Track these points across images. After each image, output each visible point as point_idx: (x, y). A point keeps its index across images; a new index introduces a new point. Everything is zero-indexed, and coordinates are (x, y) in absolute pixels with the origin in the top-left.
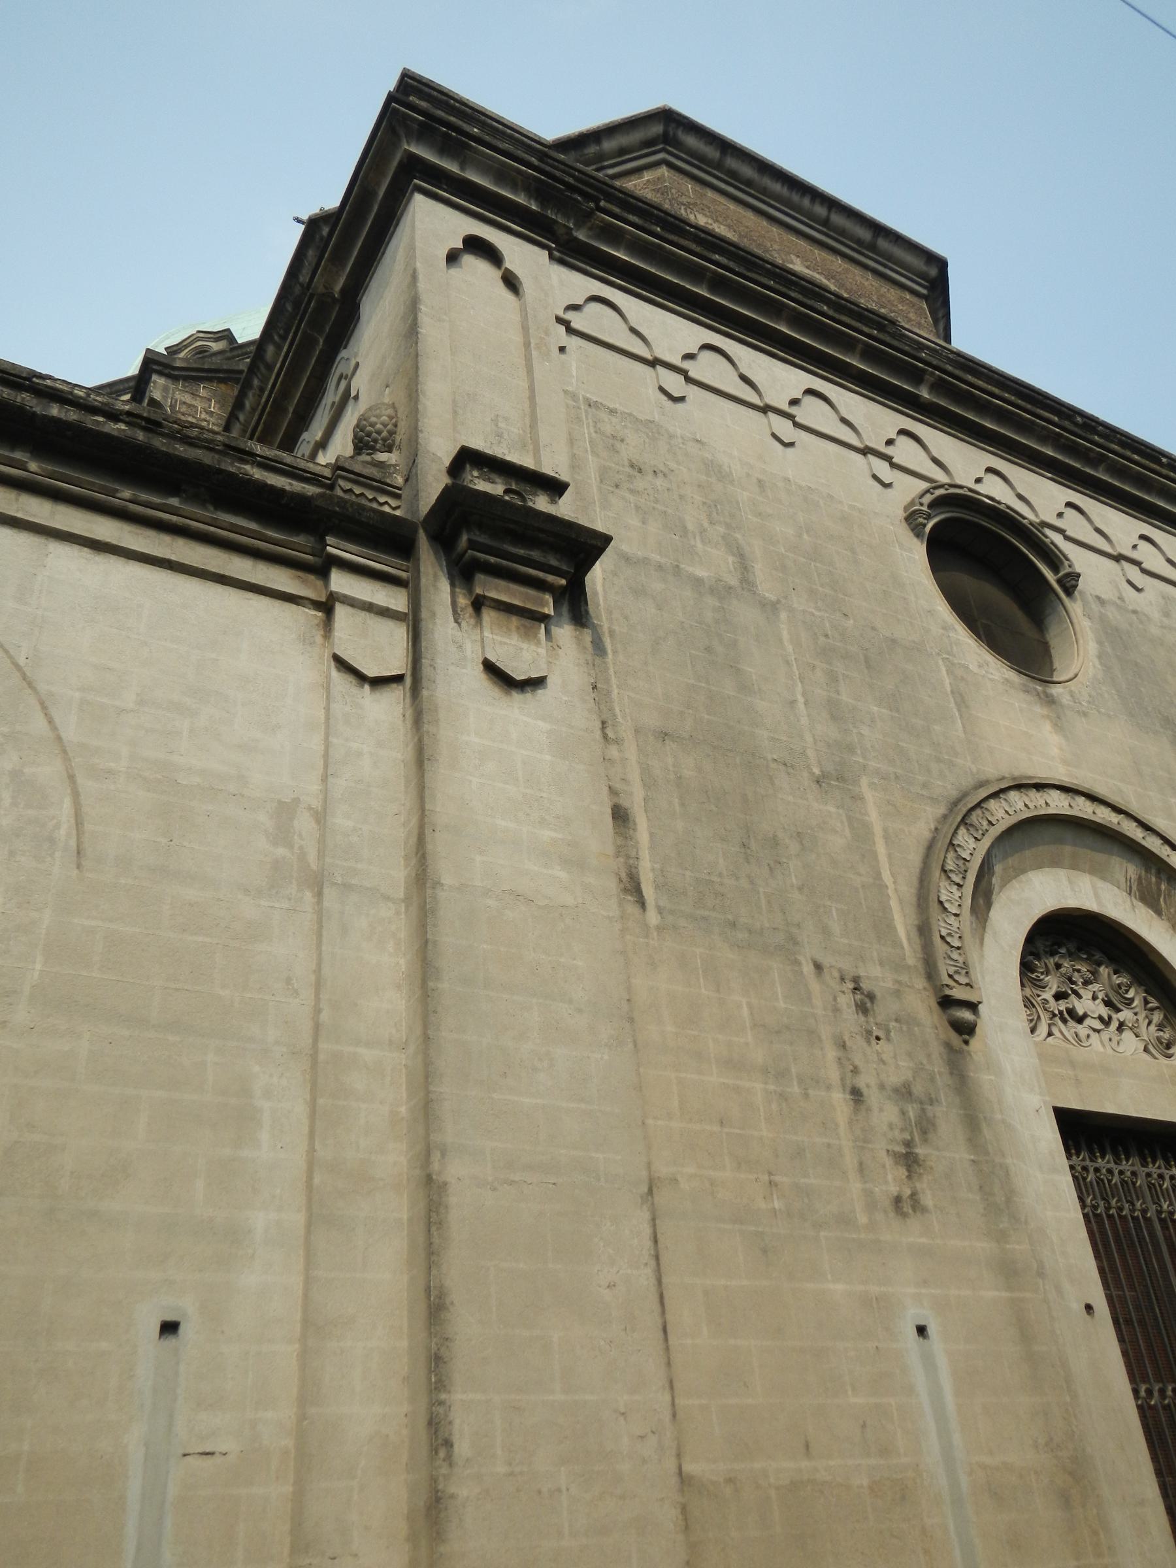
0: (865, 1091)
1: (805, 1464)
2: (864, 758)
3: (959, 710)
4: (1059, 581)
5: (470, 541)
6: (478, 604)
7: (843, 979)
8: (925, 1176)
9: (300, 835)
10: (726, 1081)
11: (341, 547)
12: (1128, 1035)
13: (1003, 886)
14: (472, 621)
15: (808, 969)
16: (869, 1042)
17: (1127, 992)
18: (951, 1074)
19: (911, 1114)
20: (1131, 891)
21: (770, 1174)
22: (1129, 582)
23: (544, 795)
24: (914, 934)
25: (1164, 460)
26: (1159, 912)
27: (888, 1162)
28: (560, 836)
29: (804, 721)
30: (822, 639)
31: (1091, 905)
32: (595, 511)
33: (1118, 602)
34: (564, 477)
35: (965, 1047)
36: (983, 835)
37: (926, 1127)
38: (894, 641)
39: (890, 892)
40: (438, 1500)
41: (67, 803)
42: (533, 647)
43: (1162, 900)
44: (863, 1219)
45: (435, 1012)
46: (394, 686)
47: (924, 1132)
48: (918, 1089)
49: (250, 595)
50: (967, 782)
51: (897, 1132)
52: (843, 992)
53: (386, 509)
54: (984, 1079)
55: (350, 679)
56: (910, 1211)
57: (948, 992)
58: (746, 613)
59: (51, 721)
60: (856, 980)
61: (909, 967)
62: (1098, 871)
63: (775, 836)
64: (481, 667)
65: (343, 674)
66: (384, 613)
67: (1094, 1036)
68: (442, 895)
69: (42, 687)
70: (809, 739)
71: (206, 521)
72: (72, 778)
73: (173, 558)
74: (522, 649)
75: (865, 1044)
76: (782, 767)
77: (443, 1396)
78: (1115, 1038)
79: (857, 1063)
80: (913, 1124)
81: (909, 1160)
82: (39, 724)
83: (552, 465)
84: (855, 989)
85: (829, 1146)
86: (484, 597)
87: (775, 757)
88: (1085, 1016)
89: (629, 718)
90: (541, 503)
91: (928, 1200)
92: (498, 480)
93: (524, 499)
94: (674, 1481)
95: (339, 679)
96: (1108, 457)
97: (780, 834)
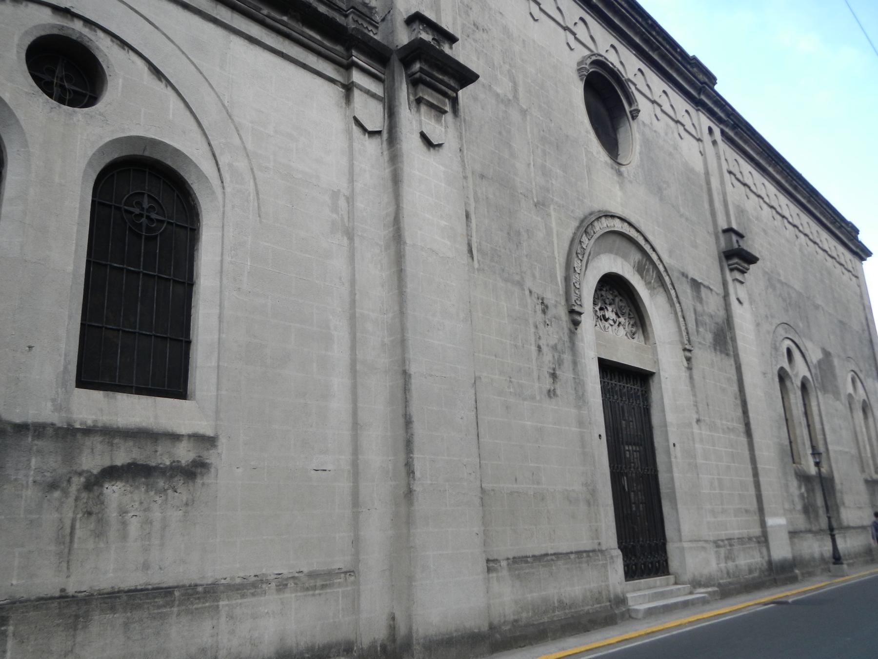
0: (542, 346)
1: (515, 486)
2: (553, 195)
3: (588, 175)
4: (631, 112)
5: (421, 68)
6: (419, 101)
7: (538, 298)
9: (341, 209)
10: (498, 338)
11: (358, 57)
12: (621, 327)
14: (415, 109)
15: (527, 293)
16: (545, 326)
17: (623, 309)
18: (570, 342)
19: (556, 357)
21: (510, 378)
22: (656, 116)
23: (442, 203)
24: (563, 281)
25: (679, 50)
26: (642, 277)
27: (547, 376)
28: (447, 224)
29: (533, 174)
30: (542, 132)
31: (620, 272)
32: (459, 50)
33: (650, 125)
34: (458, 34)
36: (591, 238)
37: (560, 362)
38: (567, 136)
39: (557, 260)
40: (411, 492)
41: (252, 183)
42: (440, 127)
44: (538, 398)
45: (405, 302)
46: (377, 136)
47: (559, 365)
48: (559, 347)
49: (315, 76)
50: (587, 211)
51: (551, 364)
52: (538, 304)
53: (371, 34)
54: (579, 344)
55: (360, 131)
57: (574, 308)
58: (515, 116)
59: (241, 138)
60: (543, 299)
61: (560, 295)
62: (625, 257)
63: (519, 230)
64: (419, 135)
65: (357, 128)
66: (374, 96)
67: (610, 327)
68: (407, 248)
69: (236, 119)
70: (534, 184)
71: (298, 32)
72: (252, 169)
73: (284, 51)
74: (436, 128)
75: (543, 327)
76: (523, 197)
77: (411, 455)
78: (617, 329)
79: (541, 335)
81: (554, 376)
82: (236, 140)
83: (446, 23)
84: (542, 303)
85: (529, 368)
86: (423, 98)
87: (522, 192)
88: (608, 318)
89: (470, 166)
90: (446, 49)
91: (558, 392)
92: (430, 33)
93: (439, 45)
94: (479, 489)
95: (356, 129)
96: (660, 48)
97: (521, 230)
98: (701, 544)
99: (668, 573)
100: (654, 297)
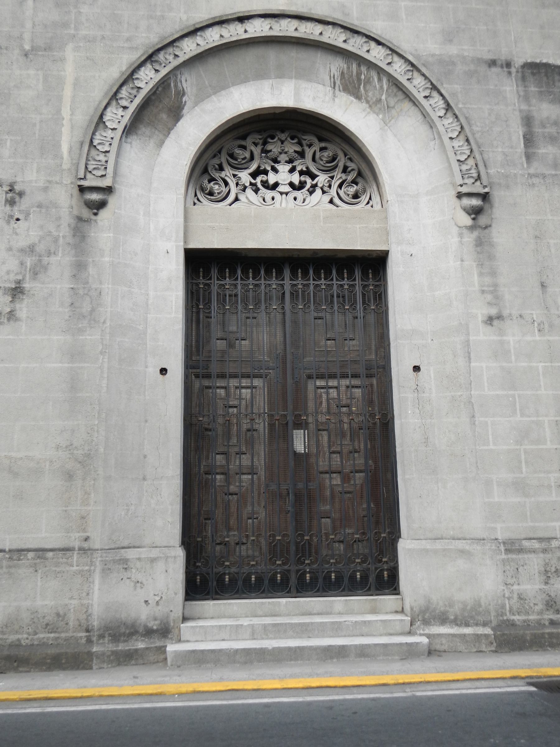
8: (26, 300)
13: (196, 104)
16: (8, 222)
26: (358, 97)
35: (93, 217)
43: (362, 87)
56: (6, 321)
80: (28, 269)
98: (460, 545)
99: (398, 594)
100: (393, 121)
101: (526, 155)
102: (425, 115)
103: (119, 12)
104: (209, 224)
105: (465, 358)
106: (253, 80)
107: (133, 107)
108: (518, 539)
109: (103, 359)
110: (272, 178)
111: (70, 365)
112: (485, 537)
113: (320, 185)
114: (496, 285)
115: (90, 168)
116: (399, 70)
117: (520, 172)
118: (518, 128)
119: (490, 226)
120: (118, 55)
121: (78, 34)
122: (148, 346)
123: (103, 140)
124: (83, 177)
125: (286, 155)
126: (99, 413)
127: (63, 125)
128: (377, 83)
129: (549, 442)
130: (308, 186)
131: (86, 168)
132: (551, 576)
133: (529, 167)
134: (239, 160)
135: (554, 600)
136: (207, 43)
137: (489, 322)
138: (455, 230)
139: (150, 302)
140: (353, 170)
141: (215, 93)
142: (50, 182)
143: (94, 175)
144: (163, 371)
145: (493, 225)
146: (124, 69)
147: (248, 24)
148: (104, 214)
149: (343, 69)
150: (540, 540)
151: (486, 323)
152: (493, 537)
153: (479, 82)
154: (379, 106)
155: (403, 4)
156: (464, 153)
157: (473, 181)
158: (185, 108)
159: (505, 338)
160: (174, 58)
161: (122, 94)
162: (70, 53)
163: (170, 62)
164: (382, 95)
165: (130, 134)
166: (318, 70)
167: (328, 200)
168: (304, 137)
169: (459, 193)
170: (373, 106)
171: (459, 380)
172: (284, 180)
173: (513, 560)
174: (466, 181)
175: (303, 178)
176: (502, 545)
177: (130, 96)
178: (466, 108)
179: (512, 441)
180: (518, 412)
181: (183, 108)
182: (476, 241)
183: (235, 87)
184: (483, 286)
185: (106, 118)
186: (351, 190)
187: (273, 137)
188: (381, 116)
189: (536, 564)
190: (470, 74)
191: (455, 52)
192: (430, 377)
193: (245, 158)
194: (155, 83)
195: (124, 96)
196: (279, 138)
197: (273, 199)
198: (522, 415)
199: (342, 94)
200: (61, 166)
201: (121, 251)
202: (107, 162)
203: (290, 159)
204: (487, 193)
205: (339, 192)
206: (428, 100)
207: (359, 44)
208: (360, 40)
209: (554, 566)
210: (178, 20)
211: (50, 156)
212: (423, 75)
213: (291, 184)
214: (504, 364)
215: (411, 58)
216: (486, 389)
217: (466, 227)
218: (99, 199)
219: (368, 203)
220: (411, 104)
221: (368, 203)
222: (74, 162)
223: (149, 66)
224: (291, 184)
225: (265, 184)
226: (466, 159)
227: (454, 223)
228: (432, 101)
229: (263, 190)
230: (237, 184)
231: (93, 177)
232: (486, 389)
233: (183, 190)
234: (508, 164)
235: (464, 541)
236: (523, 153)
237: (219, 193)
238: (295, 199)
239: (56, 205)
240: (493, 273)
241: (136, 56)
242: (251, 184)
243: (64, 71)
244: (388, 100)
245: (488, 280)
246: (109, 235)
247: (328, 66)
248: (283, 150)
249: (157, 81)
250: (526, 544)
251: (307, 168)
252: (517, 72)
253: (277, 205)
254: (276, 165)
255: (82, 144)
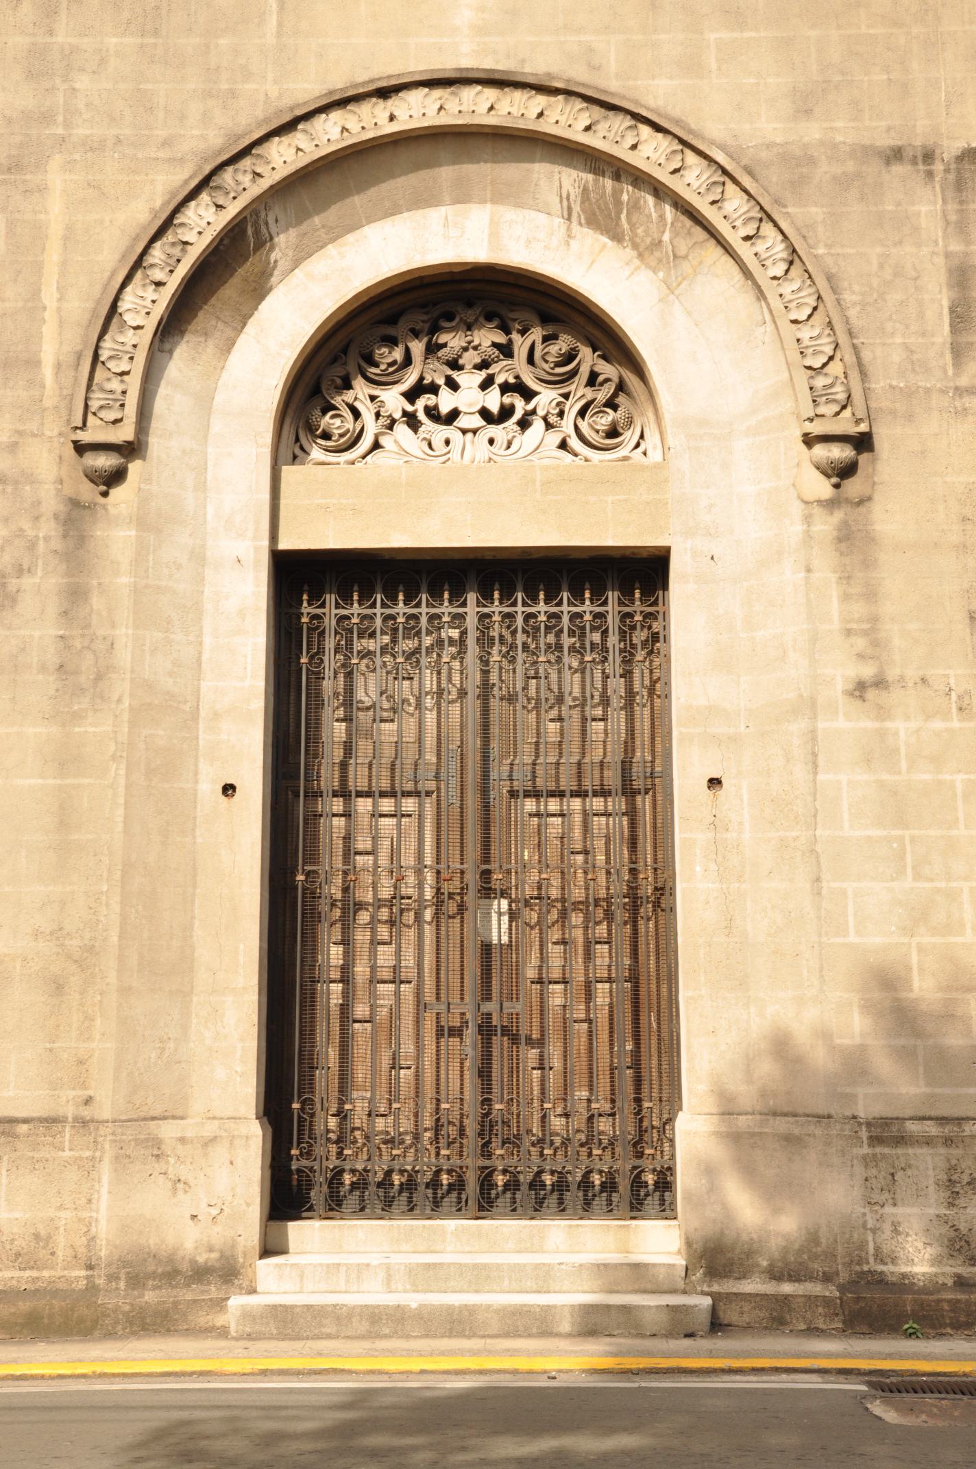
13: (296, 264)
18: (65, 536)
20: (570, 214)
26: (617, 237)
35: (102, 500)
43: (623, 216)
101: (952, 348)
102: (747, 273)
103: (150, 86)
104: (320, 501)
105: (806, 764)
106: (408, 210)
107: (174, 283)
108: (897, 1119)
109: (117, 769)
110: (446, 401)
111: (59, 781)
112: (833, 1113)
113: (541, 412)
114: (874, 619)
115: (94, 405)
116: (695, 184)
117: (938, 385)
118: (940, 292)
119: (869, 499)
120: (147, 175)
121: (70, 135)
122: (201, 743)
123: (117, 350)
124: (80, 425)
125: (476, 352)
126: (109, 870)
127: (44, 321)
128: (653, 210)
129: (969, 931)
130: (518, 414)
131: (86, 406)
132: (961, 1192)
133: (956, 374)
134: (383, 367)
135: (965, 1238)
136: (317, 146)
137: (857, 693)
138: (797, 509)
139: (205, 657)
140: (607, 380)
141: (333, 240)
142: (20, 433)
143: (101, 419)
144: (229, 789)
145: (876, 497)
146: (158, 203)
147: (397, 103)
148: (119, 493)
149: (587, 182)
150: (942, 1120)
151: (852, 694)
152: (848, 1113)
153: (862, 198)
154: (657, 254)
155: (712, 36)
156: (822, 352)
157: (836, 408)
158: (276, 273)
159: (888, 724)
160: (253, 180)
161: (154, 256)
162: (56, 177)
163: (244, 189)
164: (664, 232)
165: (169, 333)
166: (536, 185)
167: (558, 441)
168: (513, 315)
169: (806, 435)
170: (646, 254)
171: (795, 808)
172: (470, 405)
173: (884, 1156)
174: (822, 410)
175: (507, 400)
176: (864, 1128)
177: (169, 261)
178: (832, 255)
179: (893, 928)
180: (909, 870)
181: (271, 275)
182: (839, 530)
183: (373, 225)
184: (849, 622)
185: (123, 306)
186: (603, 421)
187: (450, 317)
188: (661, 274)
189: (931, 1167)
190: (843, 182)
191: (817, 136)
192: (742, 800)
193: (394, 363)
194: (215, 234)
195: (157, 261)
196: (461, 319)
197: (447, 442)
198: (917, 876)
199: (586, 230)
200: (41, 401)
201: (151, 563)
202: (124, 392)
203: (483, 361)
204: (862, 434)
205: (579, 425)
206: (753, 244)
207: (616, 133)
208: (620, 123)
209: (967, 1172)
210: (262, 98)
211: (21, 383)
212: (745, 191)
213: (485, 413)
214: (885, 777)
215: (720, 157)
216: (846, 825)
217: (819, 502)
218: (110, 466)
219: (637, 445)
220: (720, 250)
221: (637, 445)
222: (65, 392)
223: (204, 197)
224: (485, 413)
225: (432, 413)
226: (825, 365)
227: (795, 495)
228: (760, 247)
229: (428, 425)
230: (378, 415)
231: (99, 422)
232: (846, 825)
233: (268, 438)
234: (913, 370)
235: (791, 1119)
236: (948, 346)
237: (341, 436)
238: (491, 442)
239: (30, 478)
240: (871, 595)
241: (183, 177)
242: (405, 413)
243: (46, 212)
244: (676, 242)
245: (859, 609)
246: (128, 533)
247: (557, 177)
248: (469, 343)
249: (218, 229)
250: (912, 1127)
251: (517, 377)
252: (947, 171)
253: (455, 455)
254: (455, 375)
255: (79, 356)
